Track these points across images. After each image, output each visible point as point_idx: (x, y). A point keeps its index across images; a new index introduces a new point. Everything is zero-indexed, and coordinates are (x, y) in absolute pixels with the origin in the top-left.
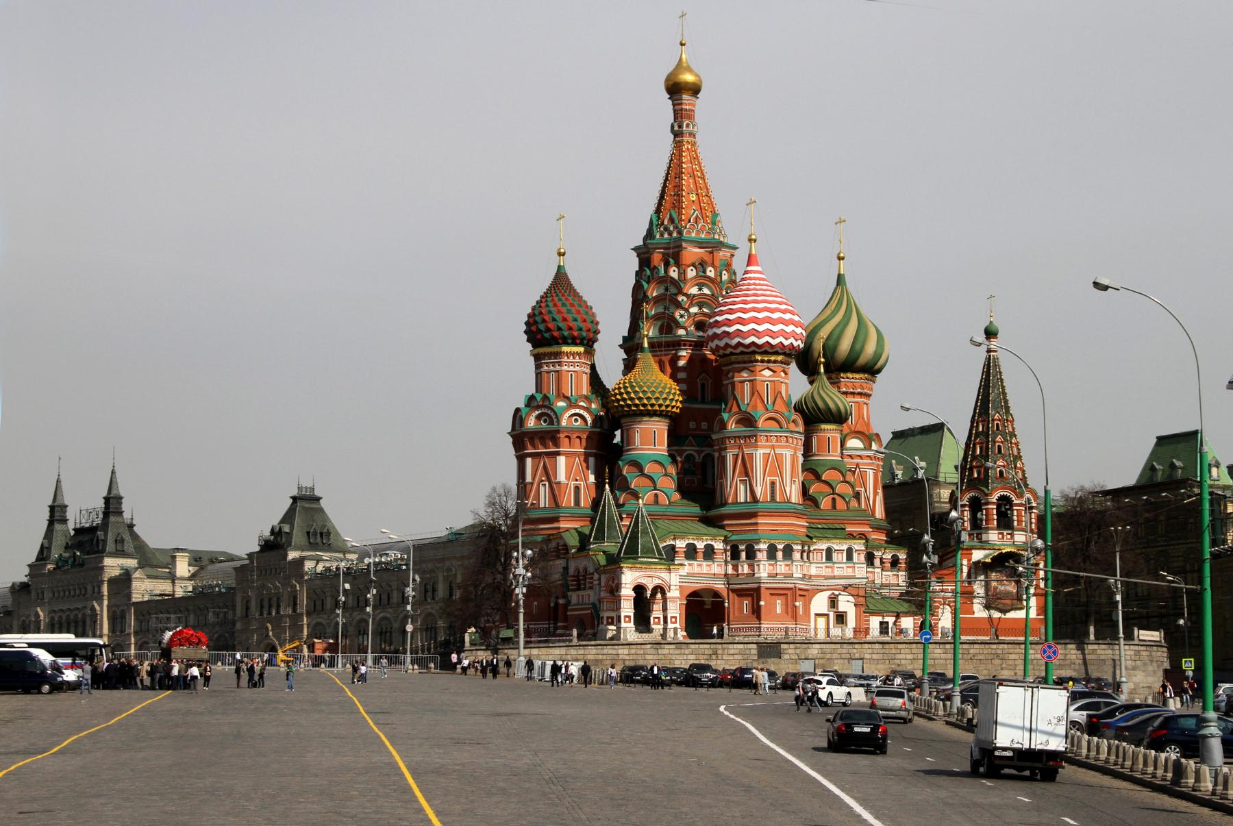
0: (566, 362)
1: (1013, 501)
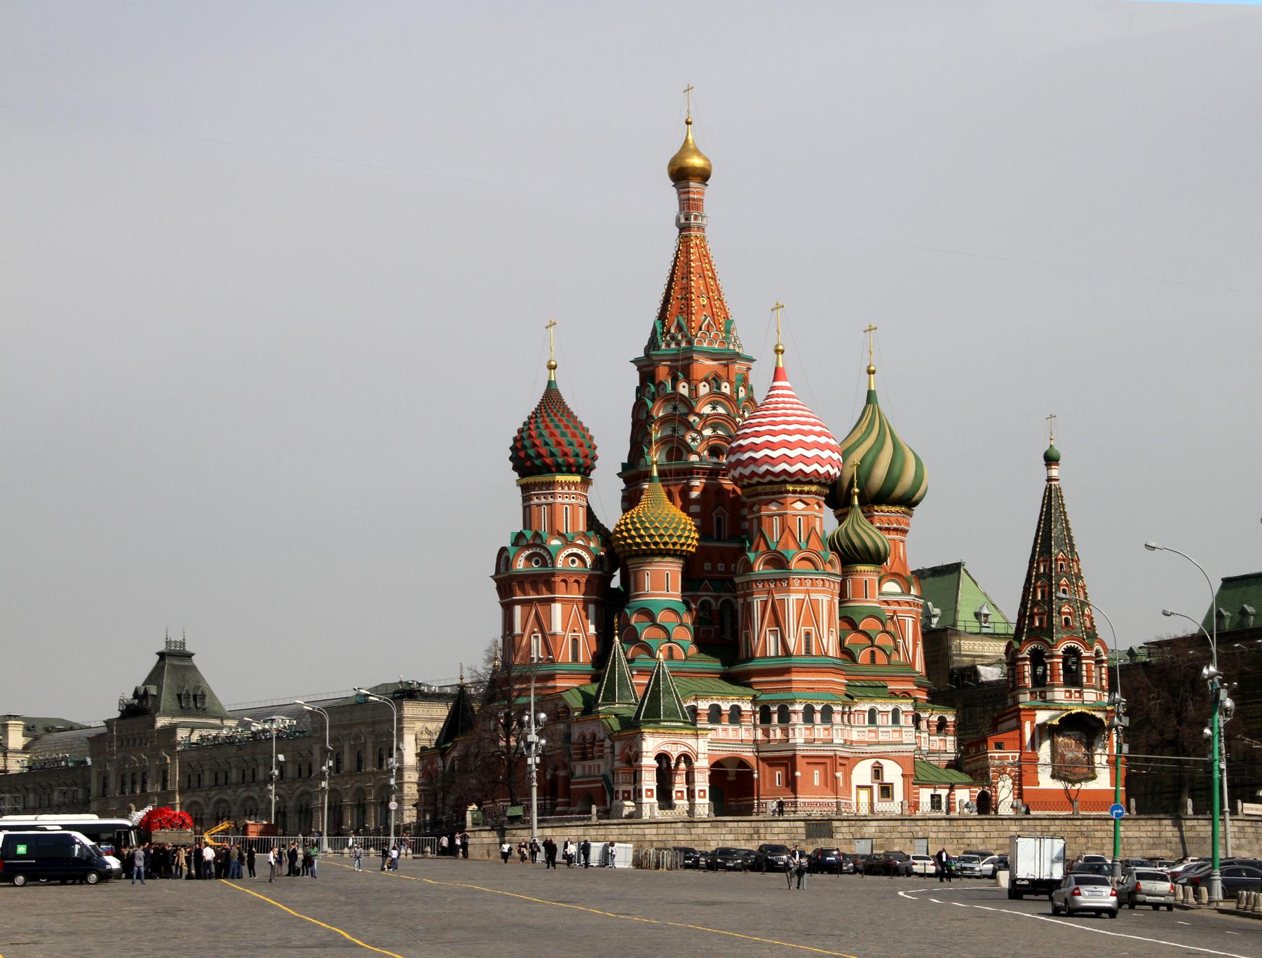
0: (559, 493)
1: (1082, 653)
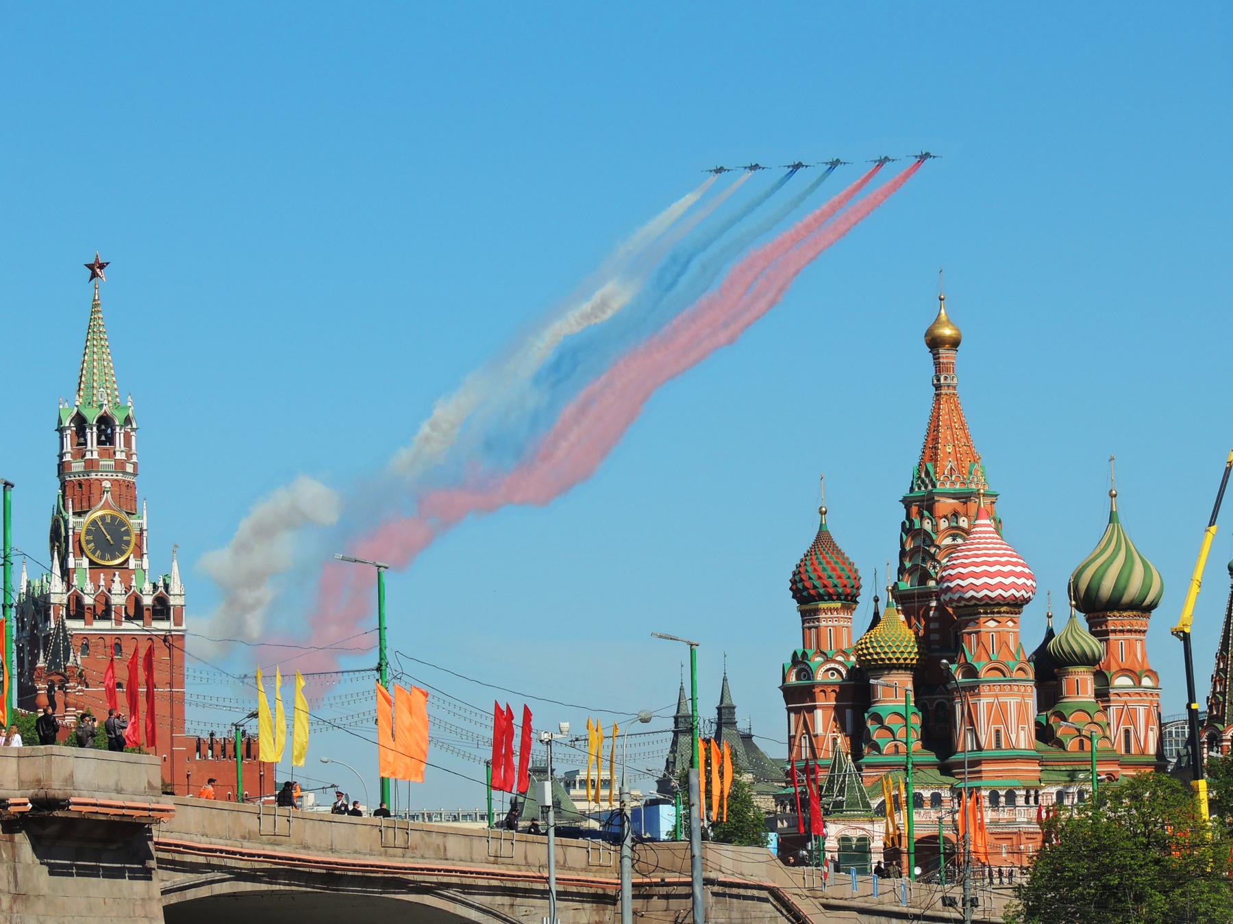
0: (823, 618)
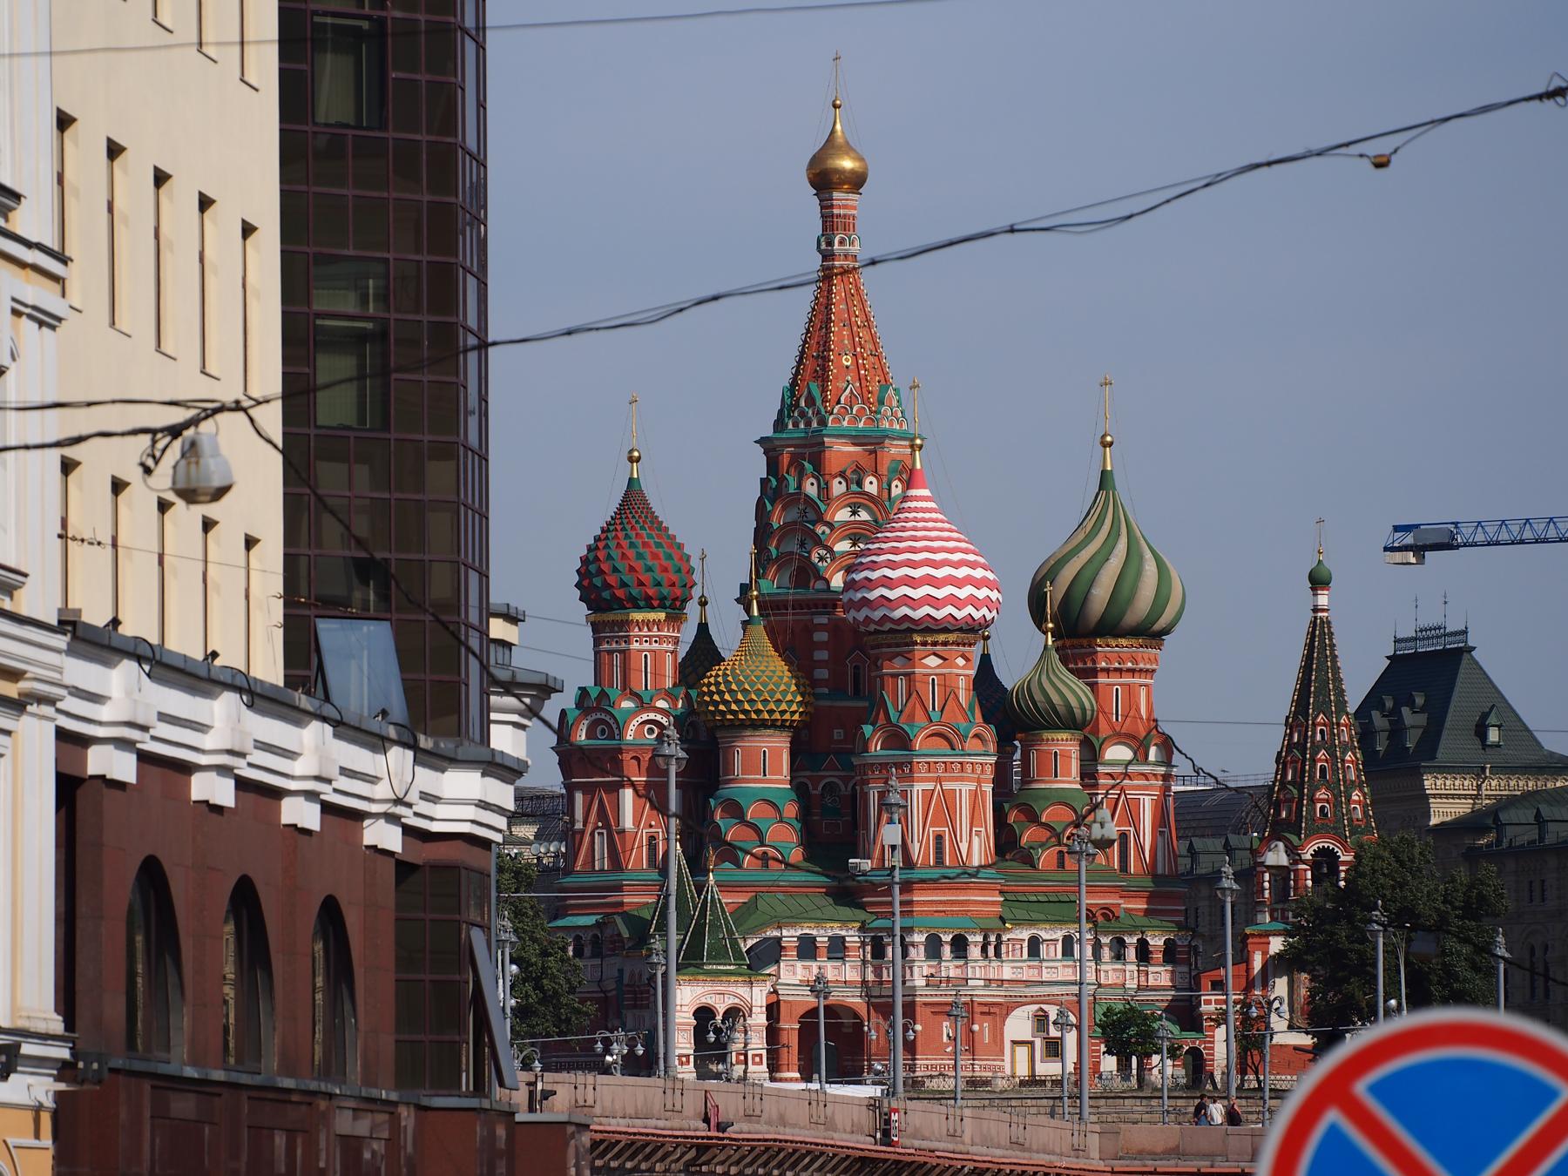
0: (635, 636)
1: (1339, 857)
